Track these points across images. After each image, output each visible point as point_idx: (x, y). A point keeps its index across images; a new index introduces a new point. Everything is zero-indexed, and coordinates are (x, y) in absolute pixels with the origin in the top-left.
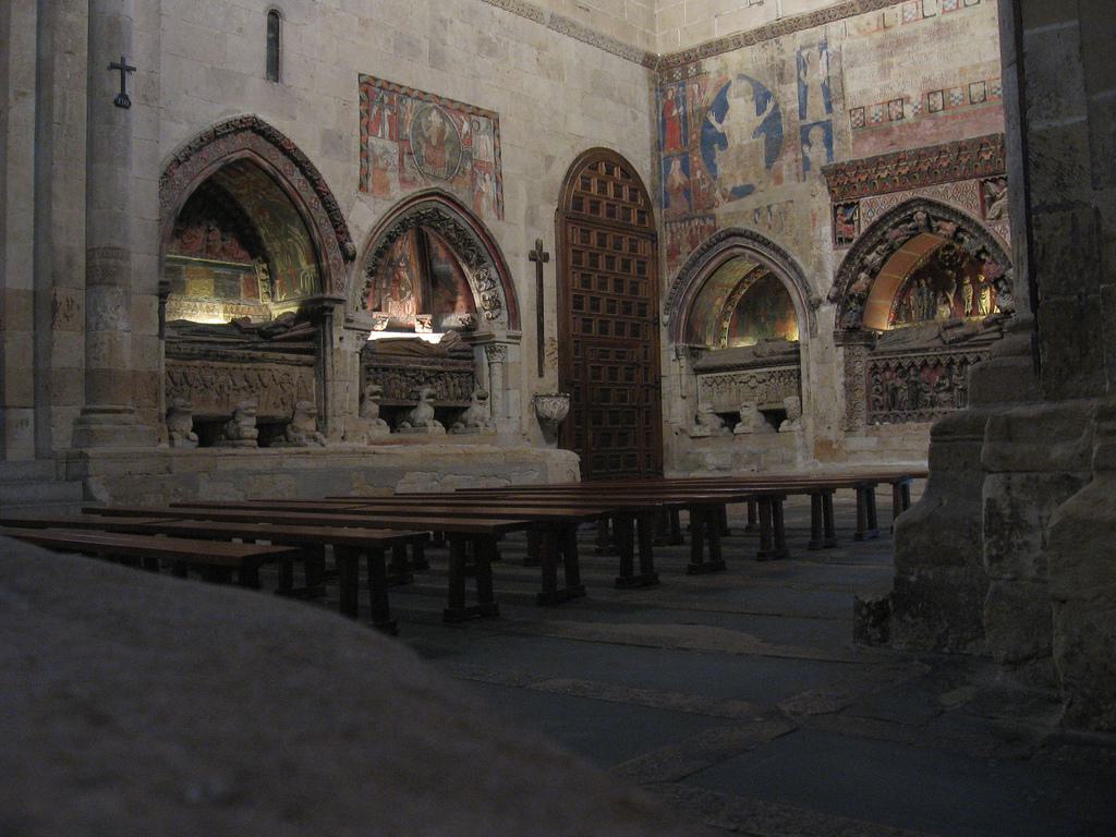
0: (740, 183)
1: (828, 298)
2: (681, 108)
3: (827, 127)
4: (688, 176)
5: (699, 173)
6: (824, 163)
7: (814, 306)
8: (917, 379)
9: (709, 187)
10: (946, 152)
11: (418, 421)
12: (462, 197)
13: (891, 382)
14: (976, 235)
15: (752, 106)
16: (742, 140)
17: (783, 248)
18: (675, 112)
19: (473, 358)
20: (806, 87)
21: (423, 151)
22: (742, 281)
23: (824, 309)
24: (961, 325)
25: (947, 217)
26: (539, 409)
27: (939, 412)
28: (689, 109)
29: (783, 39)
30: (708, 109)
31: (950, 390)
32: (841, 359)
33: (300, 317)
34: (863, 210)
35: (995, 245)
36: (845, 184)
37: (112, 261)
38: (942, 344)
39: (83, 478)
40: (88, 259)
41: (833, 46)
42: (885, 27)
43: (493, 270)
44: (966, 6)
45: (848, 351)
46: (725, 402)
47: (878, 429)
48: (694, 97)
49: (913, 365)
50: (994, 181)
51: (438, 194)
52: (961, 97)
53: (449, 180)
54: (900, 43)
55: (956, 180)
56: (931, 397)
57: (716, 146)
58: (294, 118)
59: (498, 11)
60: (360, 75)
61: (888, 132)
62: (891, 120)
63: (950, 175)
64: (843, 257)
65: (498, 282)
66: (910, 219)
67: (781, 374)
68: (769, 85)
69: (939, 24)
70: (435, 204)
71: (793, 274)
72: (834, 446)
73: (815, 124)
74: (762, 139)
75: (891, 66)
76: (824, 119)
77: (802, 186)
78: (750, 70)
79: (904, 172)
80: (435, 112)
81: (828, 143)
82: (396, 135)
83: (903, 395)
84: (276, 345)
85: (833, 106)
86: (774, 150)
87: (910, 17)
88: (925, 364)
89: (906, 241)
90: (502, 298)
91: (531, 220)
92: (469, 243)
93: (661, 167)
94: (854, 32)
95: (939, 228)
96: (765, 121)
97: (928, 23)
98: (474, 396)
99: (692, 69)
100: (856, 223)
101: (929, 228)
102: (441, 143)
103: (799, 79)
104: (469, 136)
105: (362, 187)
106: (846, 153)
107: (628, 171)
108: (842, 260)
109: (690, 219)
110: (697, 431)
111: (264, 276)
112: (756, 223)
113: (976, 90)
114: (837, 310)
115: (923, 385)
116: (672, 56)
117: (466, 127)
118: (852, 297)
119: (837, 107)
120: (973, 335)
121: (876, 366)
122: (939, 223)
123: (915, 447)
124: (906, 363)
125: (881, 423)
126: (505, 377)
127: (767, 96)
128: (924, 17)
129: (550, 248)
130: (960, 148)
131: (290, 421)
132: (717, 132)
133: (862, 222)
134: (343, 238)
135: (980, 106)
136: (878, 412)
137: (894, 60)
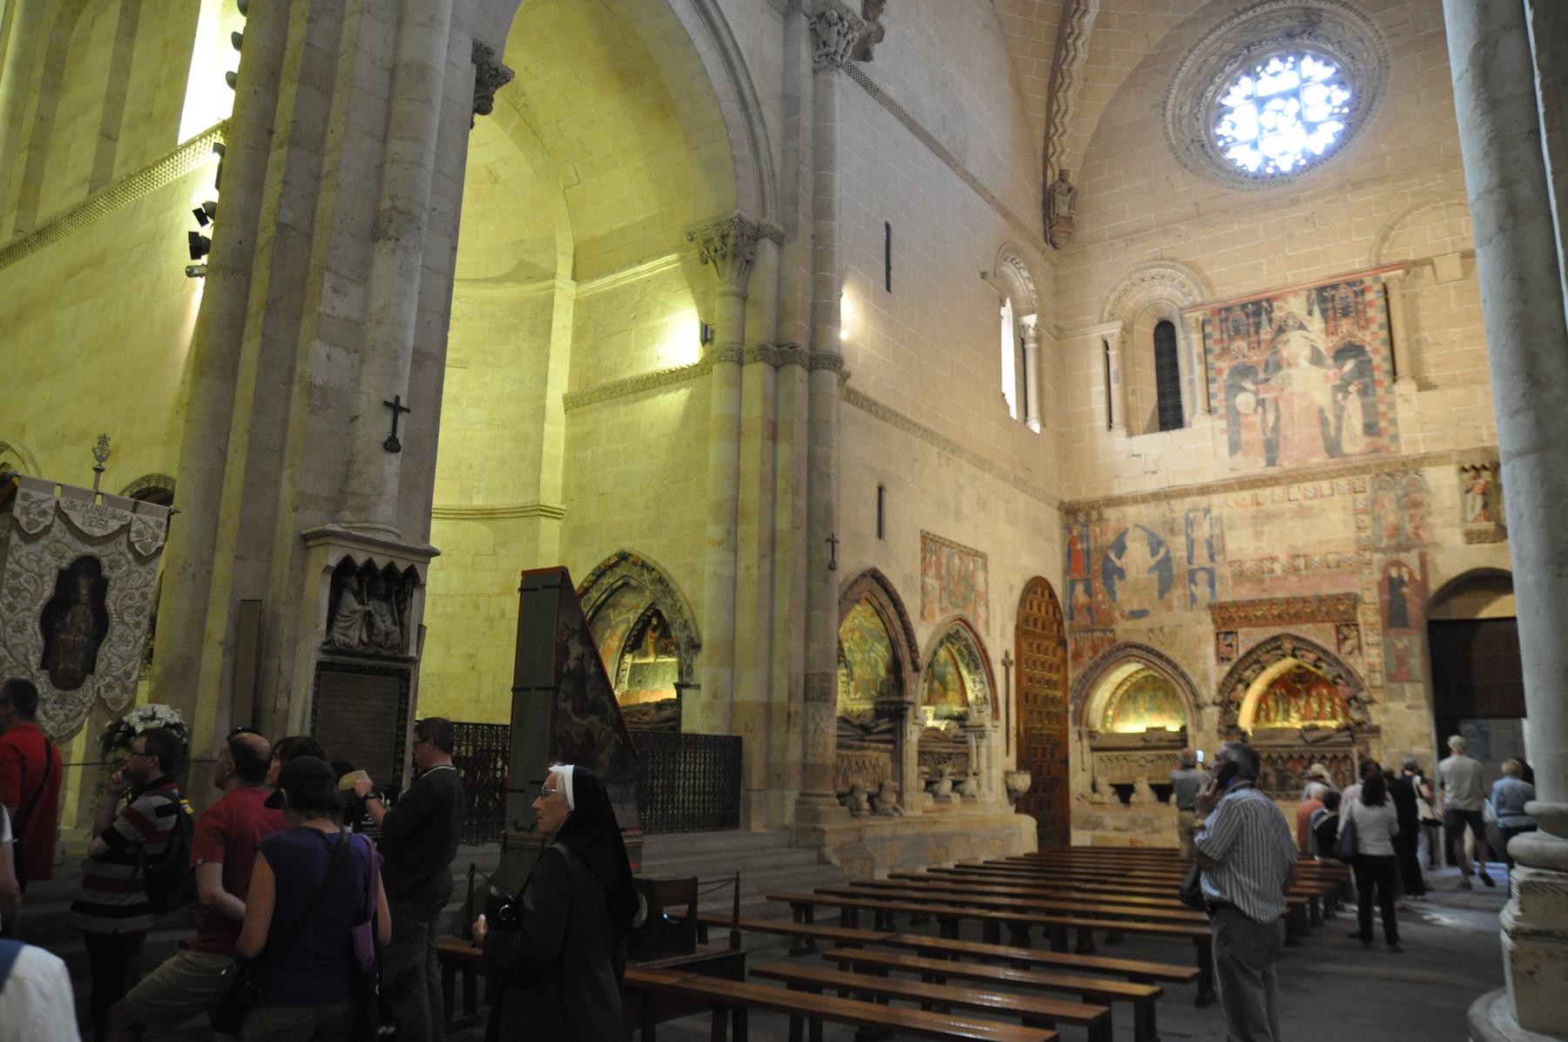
0: (1136, 607)
2: (1085, 545)
3: (1211, 573)
4: (1090, 596)
5: (1100, 597)
7: (1199, 707)
9: (1111, 606)
10: (1309, 602)
11: (942, 793)
12: (970, 619)
15: (1147, 551)
16: (1139, 574)
17: (1175, 661)
18: (1079, 546)
19: (966, 742)
20: (1193, 541)
21: (951, 587)
22: (1126, 679)
24: (1316, 728)
25: (1310, 649)
26: (1010, 782)
28: (1092, 545)
29: (1173, 502)
30: (1109, 547)
33: (879, 713)
34: (1241, 638)
35: (1349, 672)
36: (1226, 619)
37: (826, 684)
39: (819, 847)
40: (806, 681)
41: (1215, 513)
42: (1258, 504)
43: (984, 675)
44: (1322, 496)
46: (1120, 776)
48: (1096, 536)
49: (1281, 757)
50: (1347, 625)
51: (961, 620)
53: (964, 607)
54: (1270, 517)
55: (1318, 622)
57: (1115, 577)
58: (889, 566)
59: (987, 476)
60: (922, 531)
61: (1261, 581)
62: (1263, 573)
63: (1312, 618)
65: (986, 684)
66: (1279, 648)
67: (1168, 757)
68: (1163, 535)
69: (1301, 506)
70: (958, 627)
71: (1182, 682)
73: (1202, 569)
74: (1155, 575)
75: (1263, 533)
76: (1208, 565)
77: (1189, 615)
78: (1145, 522)
79: (1276, 613)
80: (956, 557)
81: (1212, 585)
82: (939, 577)
84: (874, 737)
85: (1216, 558)
86: (1165, 587)
87: (1278, 499)
88: (1291, 757)
90: (989, 697)
91: (1003, 635)
92: (971, 653)
93: (1070, 587)
94: (1233, 505)
95: (1303, 656)
96: (1159, 562)
97: (1292, 505)
98: (970, 772)
99: (1094, 515)
100: (1235, 648)
101: (1294, 656)
102: (960, 580)
103: (1187, 534)
104: (973, 572)
105: (922, 615)
106: (1226, 595)
107: (1052, 595)
108: (1224, 674)
109: (1092, 631)
110: (1097, 797)
111: (844, 679)
112: (1150, 639)
113: (1332, 558)
114: (1221, 712)
116: (1079, 504)
117: (971, 566)
118: (1231, 702)
119: (1219, 558)
122: (1303, 652)
124: (1274, 756)
126: (989, 759)
127: (1160, 543)
128: (1290, 500)
129: (1012, 657)
130: (1321, 600)
131: (878, 795)
132: (1117, 567)
134: (914, 655)
135: (1335, 570)
137: (1266, 529)
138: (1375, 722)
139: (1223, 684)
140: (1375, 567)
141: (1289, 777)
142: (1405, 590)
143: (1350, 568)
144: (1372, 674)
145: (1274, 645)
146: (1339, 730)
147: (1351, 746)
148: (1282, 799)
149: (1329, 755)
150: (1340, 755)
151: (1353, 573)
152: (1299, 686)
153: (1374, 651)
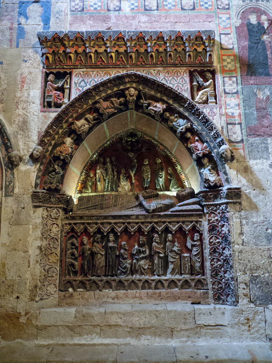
1: (31, 156)
6: (40, 29)
8: (115, 245)
13: (88, 247)
14: (187, 114)
23: (22, 167)
25: (159, 95)
27: (140, 280)
31: (150, 257)
32: (39, 221)
34: (75, 79)
35: (206, 121)
38: (144, 213)
45: (45, 213)
47: (71, 295)
49: (113, 231)
52: (174, 3)
56: (131, 264)
61: (106, 19)
62: (109, 10)
64: (51, 120)
72: (23, 320)
77: (14, 51)
83: (100, 260)
89: (114, 114)
95: (149, 105)
100: (67, 91)
114: (39, 170)
115: (122, 251)
118: (56, 158)
120: (172, 205)
121: (73, 230)
123: (120, 322)
124: (106, 229)
125: (74, 290)
133: (73, 91)
136: (72, 278)
138: (234, 185)
139: (47, 133)
140: (233, 12)
141: (121, 255)
142: (265, 37)
143: (207, 12)
144: (230, 127)
145: (115, 89)
146: (180, 198)
147: (200, 216)
148: (111, 288)
149: (174, 228)
150: (187, 227)
151: (208, 16)
152: (131, 155)
153: (233, 101)
